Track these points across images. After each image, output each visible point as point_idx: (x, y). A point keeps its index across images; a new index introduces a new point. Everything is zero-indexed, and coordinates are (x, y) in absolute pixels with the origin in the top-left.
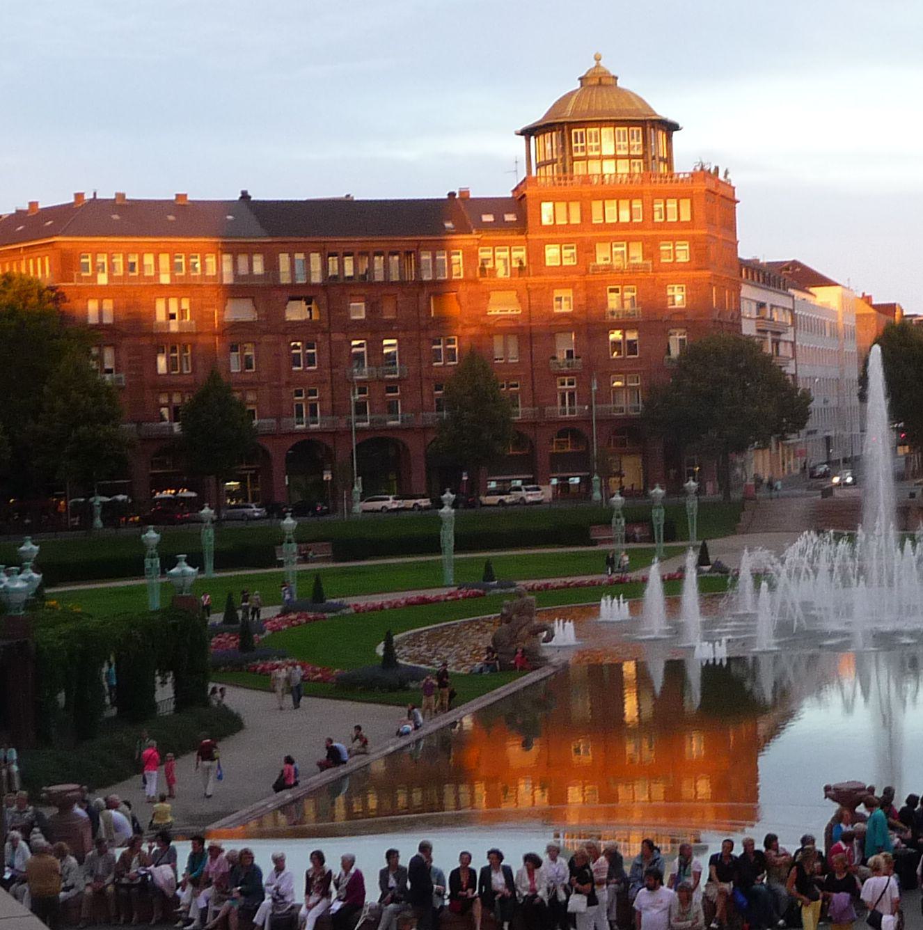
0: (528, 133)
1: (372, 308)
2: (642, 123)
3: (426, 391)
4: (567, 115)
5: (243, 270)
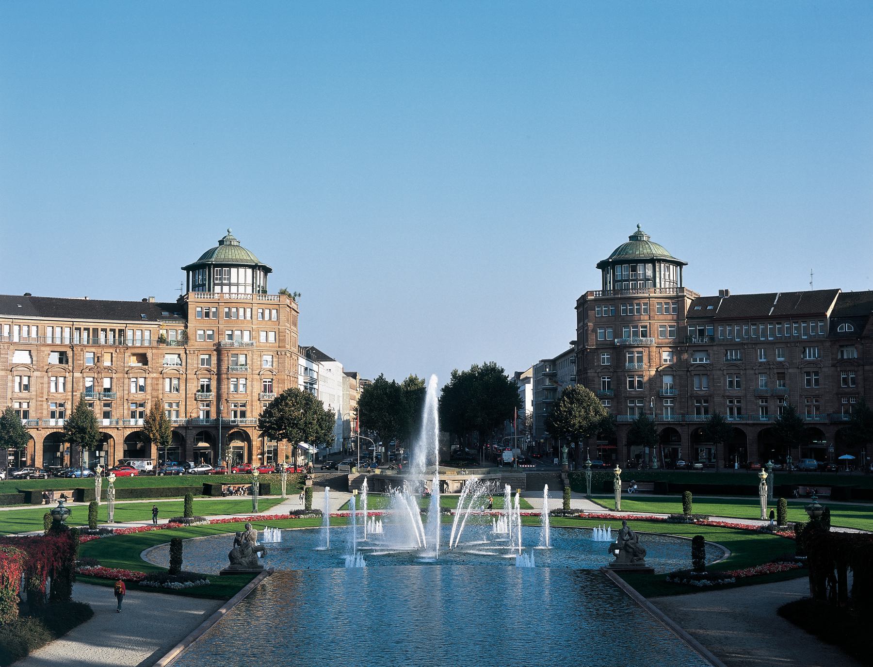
0: (188, 269)
1: (98, 359)
2: (254, 267)
3: (126, 407)
4: (213, 260)
5: (25, 334)
